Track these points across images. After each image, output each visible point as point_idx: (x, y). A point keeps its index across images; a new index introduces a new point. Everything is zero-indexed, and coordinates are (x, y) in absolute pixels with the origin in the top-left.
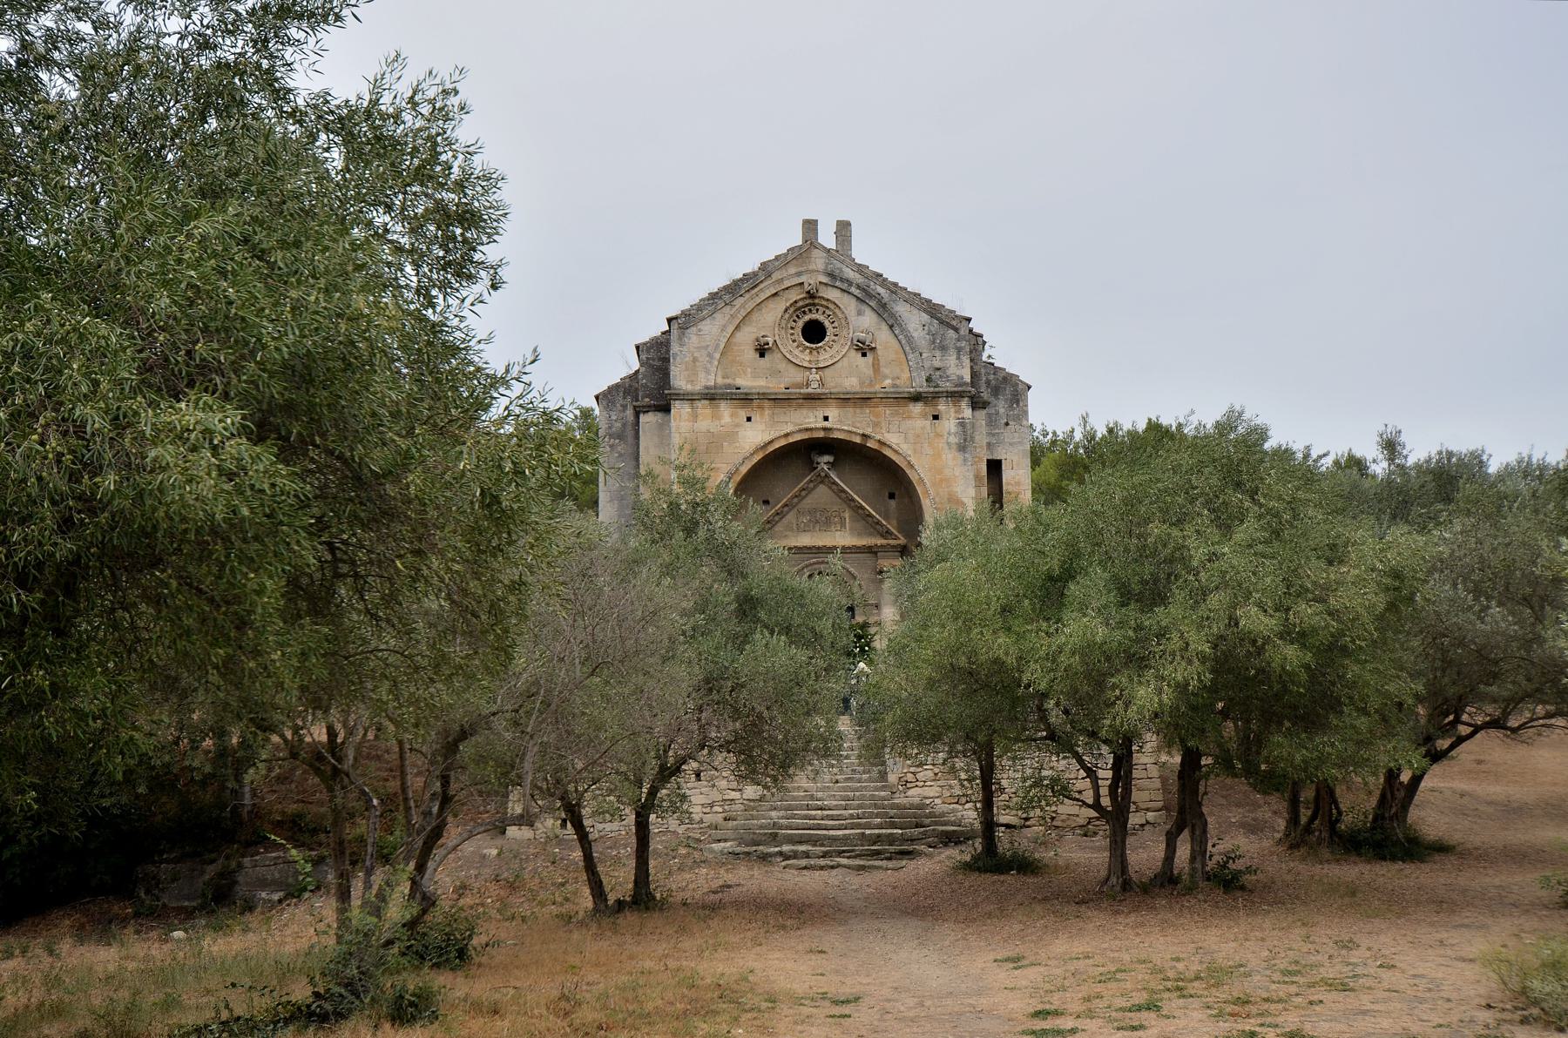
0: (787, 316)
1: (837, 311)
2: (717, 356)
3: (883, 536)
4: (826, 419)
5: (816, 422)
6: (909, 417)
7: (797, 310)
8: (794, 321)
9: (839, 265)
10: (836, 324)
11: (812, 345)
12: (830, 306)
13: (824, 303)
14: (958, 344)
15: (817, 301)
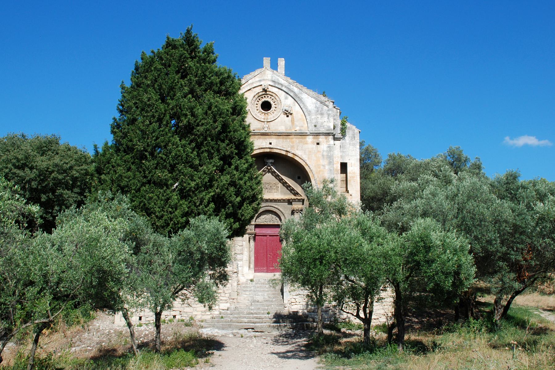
0: (255, 99)
1: (276, 97)
3: (295, 196)
4: (270, 144)
5: (266, 145)
6: (307, 144)
7: (260, 97)
8: (258, 101)
9: (278, 77)
10: (276, 103)
12: (273, 95)
13: (271, 93)
14: (328, 112)
15: (268, 93)
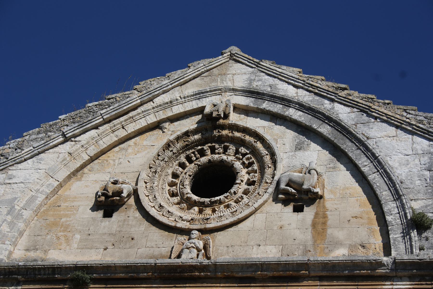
2: (26, 214)
8: (182, 165)
11: (202, 200)
